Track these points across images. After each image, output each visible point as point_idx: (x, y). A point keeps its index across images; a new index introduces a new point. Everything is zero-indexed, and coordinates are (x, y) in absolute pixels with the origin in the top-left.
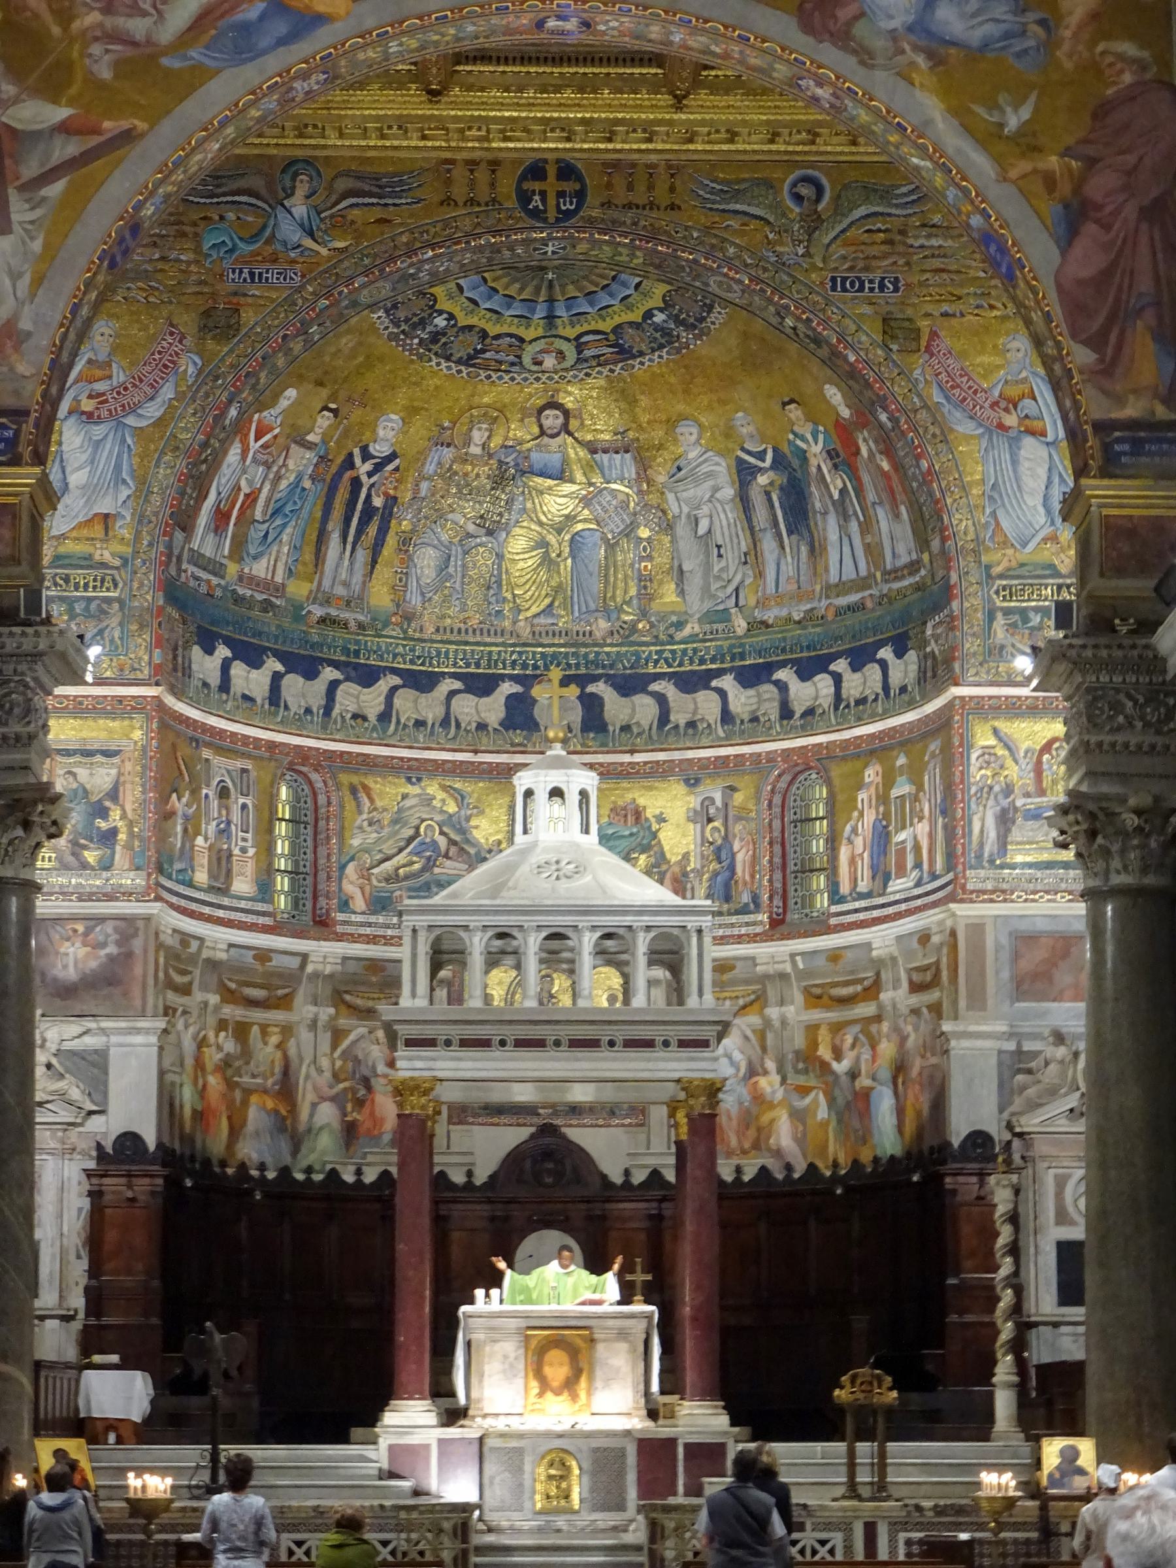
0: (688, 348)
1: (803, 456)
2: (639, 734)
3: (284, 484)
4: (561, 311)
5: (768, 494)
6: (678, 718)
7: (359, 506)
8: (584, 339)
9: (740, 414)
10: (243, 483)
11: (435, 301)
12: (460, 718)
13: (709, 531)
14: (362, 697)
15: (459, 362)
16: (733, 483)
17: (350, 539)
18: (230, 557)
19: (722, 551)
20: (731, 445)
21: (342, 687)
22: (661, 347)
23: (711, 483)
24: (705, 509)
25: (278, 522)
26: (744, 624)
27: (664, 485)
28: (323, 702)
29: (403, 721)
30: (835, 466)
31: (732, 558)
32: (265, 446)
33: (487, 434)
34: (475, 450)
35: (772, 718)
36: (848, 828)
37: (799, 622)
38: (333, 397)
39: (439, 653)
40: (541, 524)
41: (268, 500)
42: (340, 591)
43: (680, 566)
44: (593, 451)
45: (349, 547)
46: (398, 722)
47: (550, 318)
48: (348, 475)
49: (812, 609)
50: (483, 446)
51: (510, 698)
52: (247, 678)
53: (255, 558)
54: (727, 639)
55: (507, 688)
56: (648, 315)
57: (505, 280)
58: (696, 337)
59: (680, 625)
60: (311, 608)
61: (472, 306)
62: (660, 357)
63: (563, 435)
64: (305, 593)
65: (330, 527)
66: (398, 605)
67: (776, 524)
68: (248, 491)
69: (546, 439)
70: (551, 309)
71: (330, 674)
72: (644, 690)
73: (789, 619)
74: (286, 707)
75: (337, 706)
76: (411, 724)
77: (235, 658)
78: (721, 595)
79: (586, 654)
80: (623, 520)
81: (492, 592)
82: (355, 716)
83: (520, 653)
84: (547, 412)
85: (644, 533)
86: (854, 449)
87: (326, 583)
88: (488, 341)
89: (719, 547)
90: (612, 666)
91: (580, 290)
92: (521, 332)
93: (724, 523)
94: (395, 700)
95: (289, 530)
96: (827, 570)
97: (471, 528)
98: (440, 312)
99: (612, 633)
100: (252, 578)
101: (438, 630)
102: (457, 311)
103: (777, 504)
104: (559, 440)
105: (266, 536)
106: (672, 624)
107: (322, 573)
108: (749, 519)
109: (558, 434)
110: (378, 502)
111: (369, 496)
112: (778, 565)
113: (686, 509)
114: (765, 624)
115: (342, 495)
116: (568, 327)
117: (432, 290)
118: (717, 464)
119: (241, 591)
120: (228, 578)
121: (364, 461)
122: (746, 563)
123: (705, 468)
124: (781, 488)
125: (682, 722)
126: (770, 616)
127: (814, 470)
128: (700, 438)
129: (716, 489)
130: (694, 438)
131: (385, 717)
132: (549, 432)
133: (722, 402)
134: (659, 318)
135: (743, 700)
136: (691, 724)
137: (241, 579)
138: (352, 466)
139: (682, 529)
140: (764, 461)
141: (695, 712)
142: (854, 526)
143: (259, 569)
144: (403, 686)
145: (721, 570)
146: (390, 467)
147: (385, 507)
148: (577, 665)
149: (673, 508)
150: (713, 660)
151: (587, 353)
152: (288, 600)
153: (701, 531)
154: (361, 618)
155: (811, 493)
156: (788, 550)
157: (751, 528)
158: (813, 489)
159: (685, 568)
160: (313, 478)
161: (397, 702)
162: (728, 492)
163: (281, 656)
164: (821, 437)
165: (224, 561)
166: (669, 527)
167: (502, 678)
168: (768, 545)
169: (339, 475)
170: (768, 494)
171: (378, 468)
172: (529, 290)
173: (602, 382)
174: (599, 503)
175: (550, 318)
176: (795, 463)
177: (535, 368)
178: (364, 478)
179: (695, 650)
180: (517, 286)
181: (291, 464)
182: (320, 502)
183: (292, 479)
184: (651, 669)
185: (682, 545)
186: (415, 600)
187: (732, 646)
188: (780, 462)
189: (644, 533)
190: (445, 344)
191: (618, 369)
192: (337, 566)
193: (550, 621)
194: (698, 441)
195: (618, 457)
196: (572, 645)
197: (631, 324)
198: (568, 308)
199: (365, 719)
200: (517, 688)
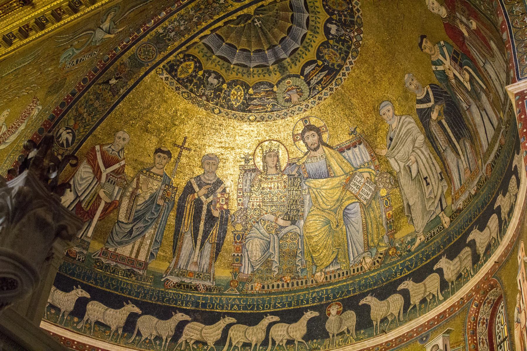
0: (360, 45)
1: (443, 76)
2: (392, 321)
3: (141, 201)
4: (283, 55)
5: (440, 123)
6: (415, 300)
7: (203, 217)
8: (305, 73)
9: (407, 76)
10: (102, 194)
11: (200, 62)
12: (275, 339)
13: (418, 170)
14: (204, 330)
15: (238, 109)
16: (421, 130)
17: (200, 237)
18: (94, 237)
19: (428, 180)
20: (410, 104)
21: (189, 325)
22: (347, 53)
23: (411, 137)
24: (412, 158)
25: (141, 225)
26: (447, 219)
27: (386, 156)
28: (172, 334)
29: (234, 344)
30: (461, 66)
31: (433, 180)
32: (116, 172)
33: (276, 158)
34: (272, 171)
35: (468, 268)
36: (516, 311)
37: (476, 194)
38: (160, 141)
39: (264, 301)
40: (323, 210)
41: (130, 210)
42: (192, 268)
43: (408, 204)
44: (341, 151)
45: (199, 243)
46: (230, 345)
47: (279, 61)
48: (190, 198)
49: (480, 179)
50: (276, 166)
51: (311, 322)
52: (104, 313)
53: (120, 243)
54: (439, 235)
55: (309, 315)
56: (327, 31)
57: (233, 35)
58: (360, 32)
59: (413, 241)
60: (168, 277)
61: (226, 64)
62: (351, 63)
63: (322, 148)
64: (164, 269)
65: (183, 229)
66: (235, 276)
67: (450, 141)
68: (109, 201)
69: (312, 153)
70: (275, 54)
71: (180, 317)
72: (395, 292)
73: (471, 197)
74: (139, 334)
75: (184, 335)
76: (239, 346)
77: (93, 298)
78: (432, 209)
79: (360, 281)
80: (370, 189)
81: (298, 259)
82: (197, 342)
83: (318, 292)
84: (307, 134)
85: (383, 192)
86: (461, 39)
87: (182, 263)
88: (251, 91)
89: (425, 179)
90: (375, 284)
91: (282, 30)
92: (267, 78)
93: (425, 160)
94: (230, 332)
95: (151, 231)
96: (481, 146)
97: (281, 222)
98: (209, 73)
99: (374, 264)
100: (118, 255)
101: (263, 287)
102: (218, 69)
103: (446, 126)
104: (320, 150)
105: (131, 232)
106: (409, 243)
107: (178, 257)
108: (436, 148)
109: (318, 147)
110: (216, 214)
111: (209, 211)
112: (458, 166)
113: (402, 165)
114: (459, 211)
115: (189, 208)
116: (293, 65)
117: (190, 52)
118: (410, 123)
119: (103, 260)
120: (90, 251)
121: (200, 187)
122: (442, 179)
123: (404, 130)
124: (445, 112)
125: (417, 302)
126: (460, 204)
127: (453, 81)
128: (394, 110)
129: (414, 141)
130: (391, 111)
131: (221, 342)
132: (313, 147)
133: (395, 76)
134: (333, 29)
135: (452, 268)
136: (424, 301)
137: (105, 253)
138: (193, 191)
139: (403, 180)
140: (430, 101)
141: (425, 291)
142: (484, 98)
143: (125, 251)
144: (238, 323)
145: (431, 192)
146: (220, 190)
147: (222, 217)
148: (354, 290)
149: (396, 167)
150: (434, 253)
151: (313, 82)
152: (149, 272)
153: (414, 174)
154: (208, 283)
155: (459, 100)
156: (460, 152)
157: (439, 154)
158: (459, 97)
159: (410, 204)
160: (163, 198)
161: (231, 333)
162: (421, 138)
163: (136, 303)
164: (445, 49)
165: (89, 240)
166: (396, 183)
167: (306, 309)
168: (450, 157)
169: (183, 199)
170: (440, 123)
171: (212, 192)
172: (253, 40)
173: (329, 100)
174: (355, 184)
175: (279, 61)
176: (443, 85)
177: (288, 104)
178: (203, 199)
179: (423, 253)
180: (244, 39)
181: (144, 187)
182: (173, 214)
183: (147, 197)
184: (399, 277)
185: (405, 188)
186: (247, 270)
187: (445, 237)
188: (439, 95)
189: (383, 192)
190: (224, 98)
191: (333, 86)
192: (190, 254)
193: (336, 267)
194: (394, 114)
195: (357, 150)
196: (351, 279)
197: (322, 44)
198: (285, 49)
199: (205, 344)
200: (316, 314)
